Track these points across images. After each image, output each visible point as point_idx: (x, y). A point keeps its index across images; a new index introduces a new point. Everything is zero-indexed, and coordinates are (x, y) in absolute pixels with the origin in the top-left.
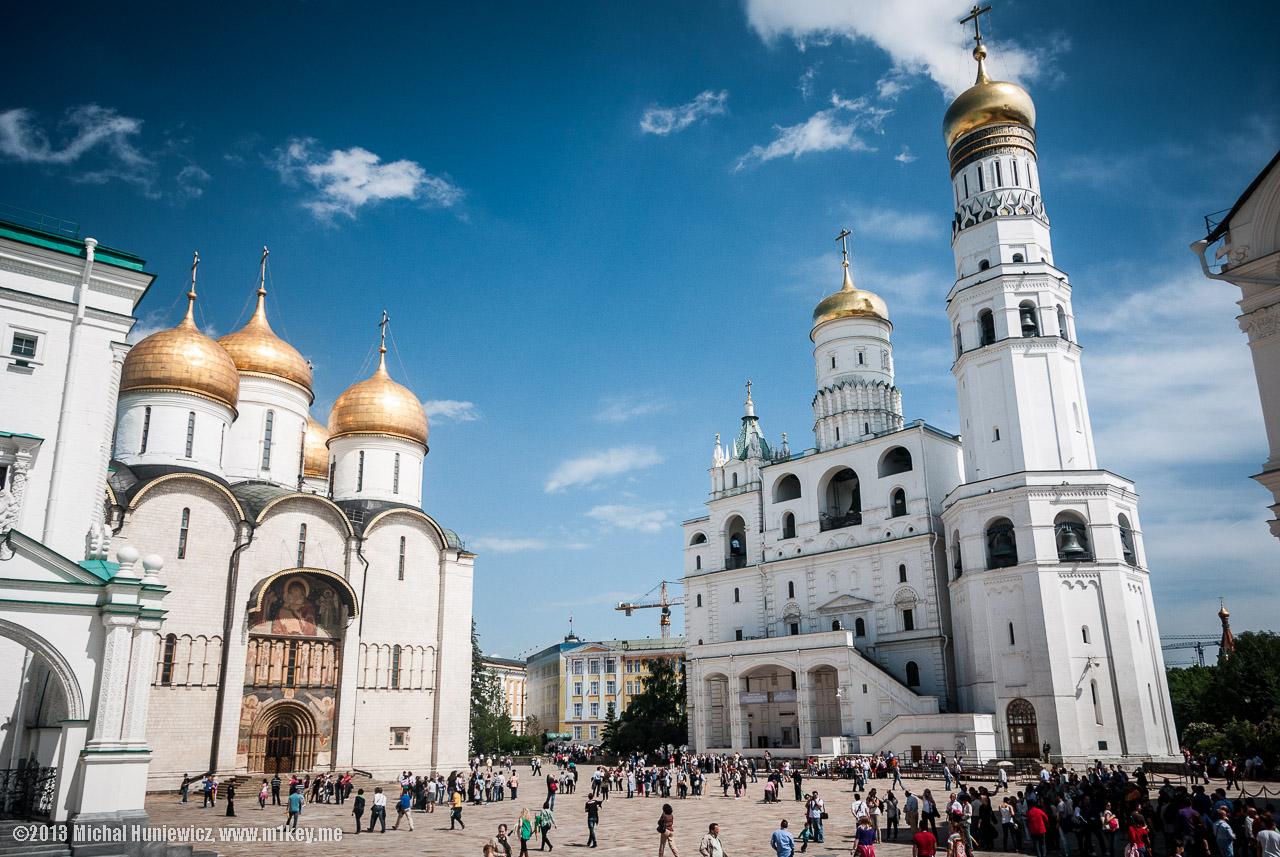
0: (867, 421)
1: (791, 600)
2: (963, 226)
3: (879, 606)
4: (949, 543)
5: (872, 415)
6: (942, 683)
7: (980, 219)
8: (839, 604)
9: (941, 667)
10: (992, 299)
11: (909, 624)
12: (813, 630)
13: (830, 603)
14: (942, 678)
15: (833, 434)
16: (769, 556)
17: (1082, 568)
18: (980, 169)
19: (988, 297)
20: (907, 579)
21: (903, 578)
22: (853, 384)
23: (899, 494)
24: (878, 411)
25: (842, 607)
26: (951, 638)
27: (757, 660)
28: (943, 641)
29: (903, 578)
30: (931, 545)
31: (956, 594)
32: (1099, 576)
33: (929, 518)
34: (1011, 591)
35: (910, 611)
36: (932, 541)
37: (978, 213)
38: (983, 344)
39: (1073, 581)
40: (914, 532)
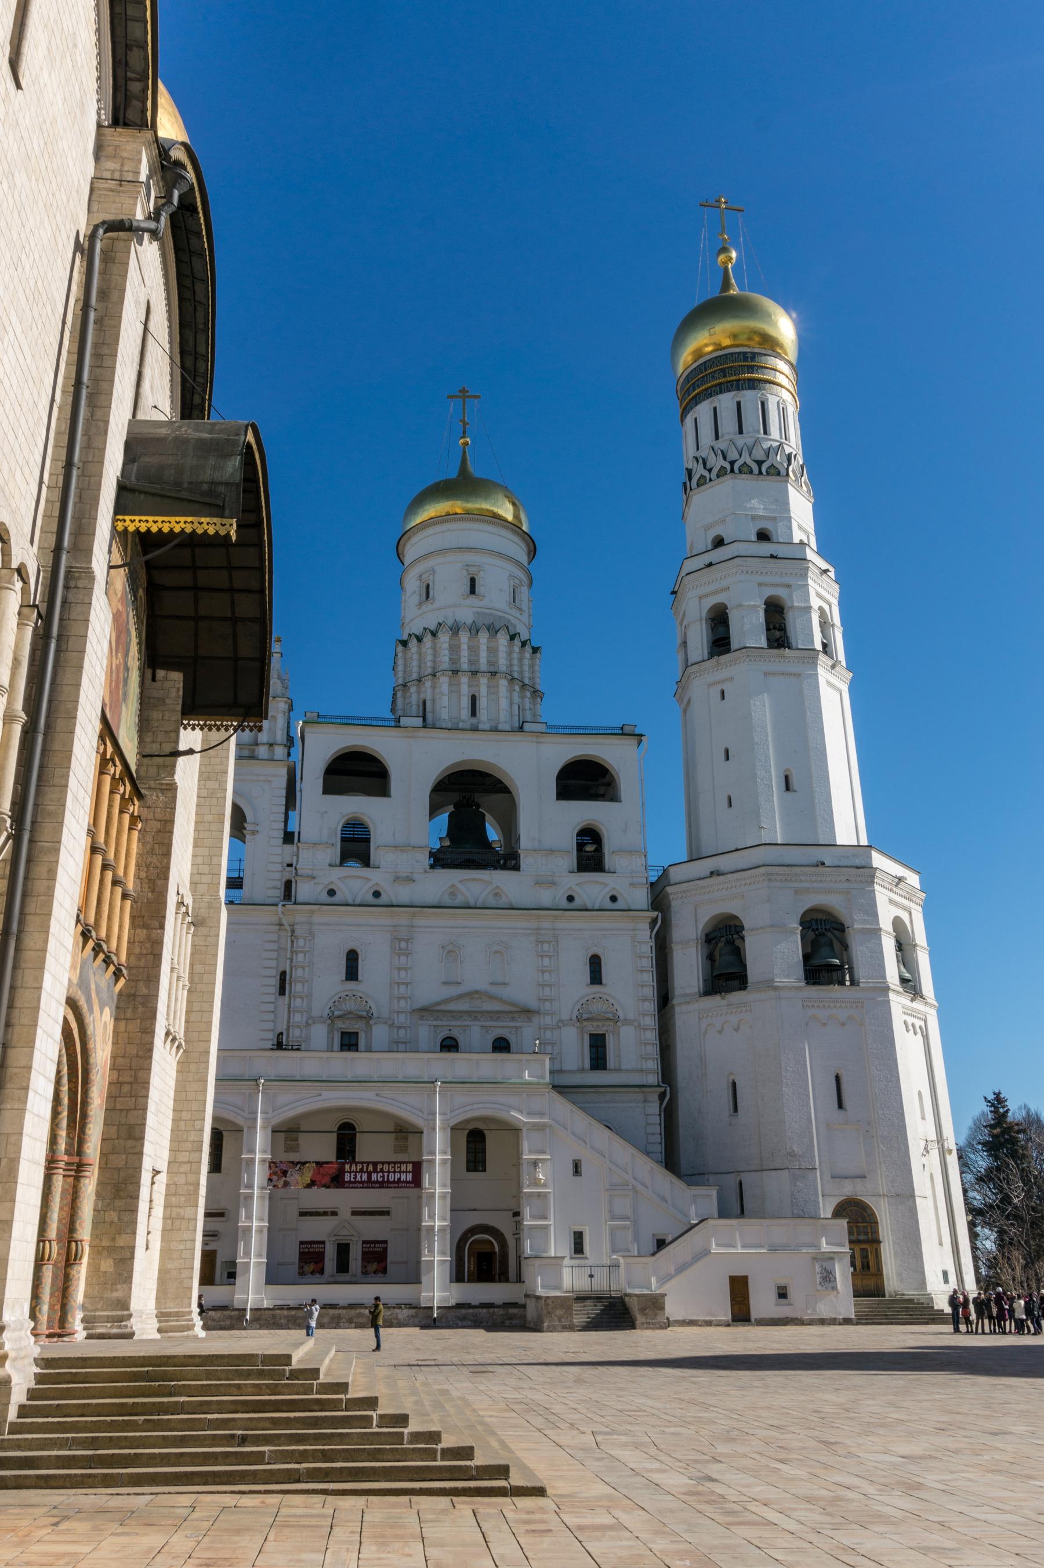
1: (351, 985)
2: (736, 468)
3: (548, 1020)
8: (463, 1006)
10: (789, 586)
11: (598, 1059)
12: (396, 1046)
13: (438, 1004)
15: (466, 702)
16: (303, 890)
17: (917, 1005)
19: (786, 580)
21: (596, 976)
25: (468, 1013)
27: (326, 1094)
28: (662, 1096)
29: (596, 976)
30: (651, 932)
34: (843, 1024)
37: (764, 462)
38: (771, 646)
39: (910, 1020)
40: (619, 905)
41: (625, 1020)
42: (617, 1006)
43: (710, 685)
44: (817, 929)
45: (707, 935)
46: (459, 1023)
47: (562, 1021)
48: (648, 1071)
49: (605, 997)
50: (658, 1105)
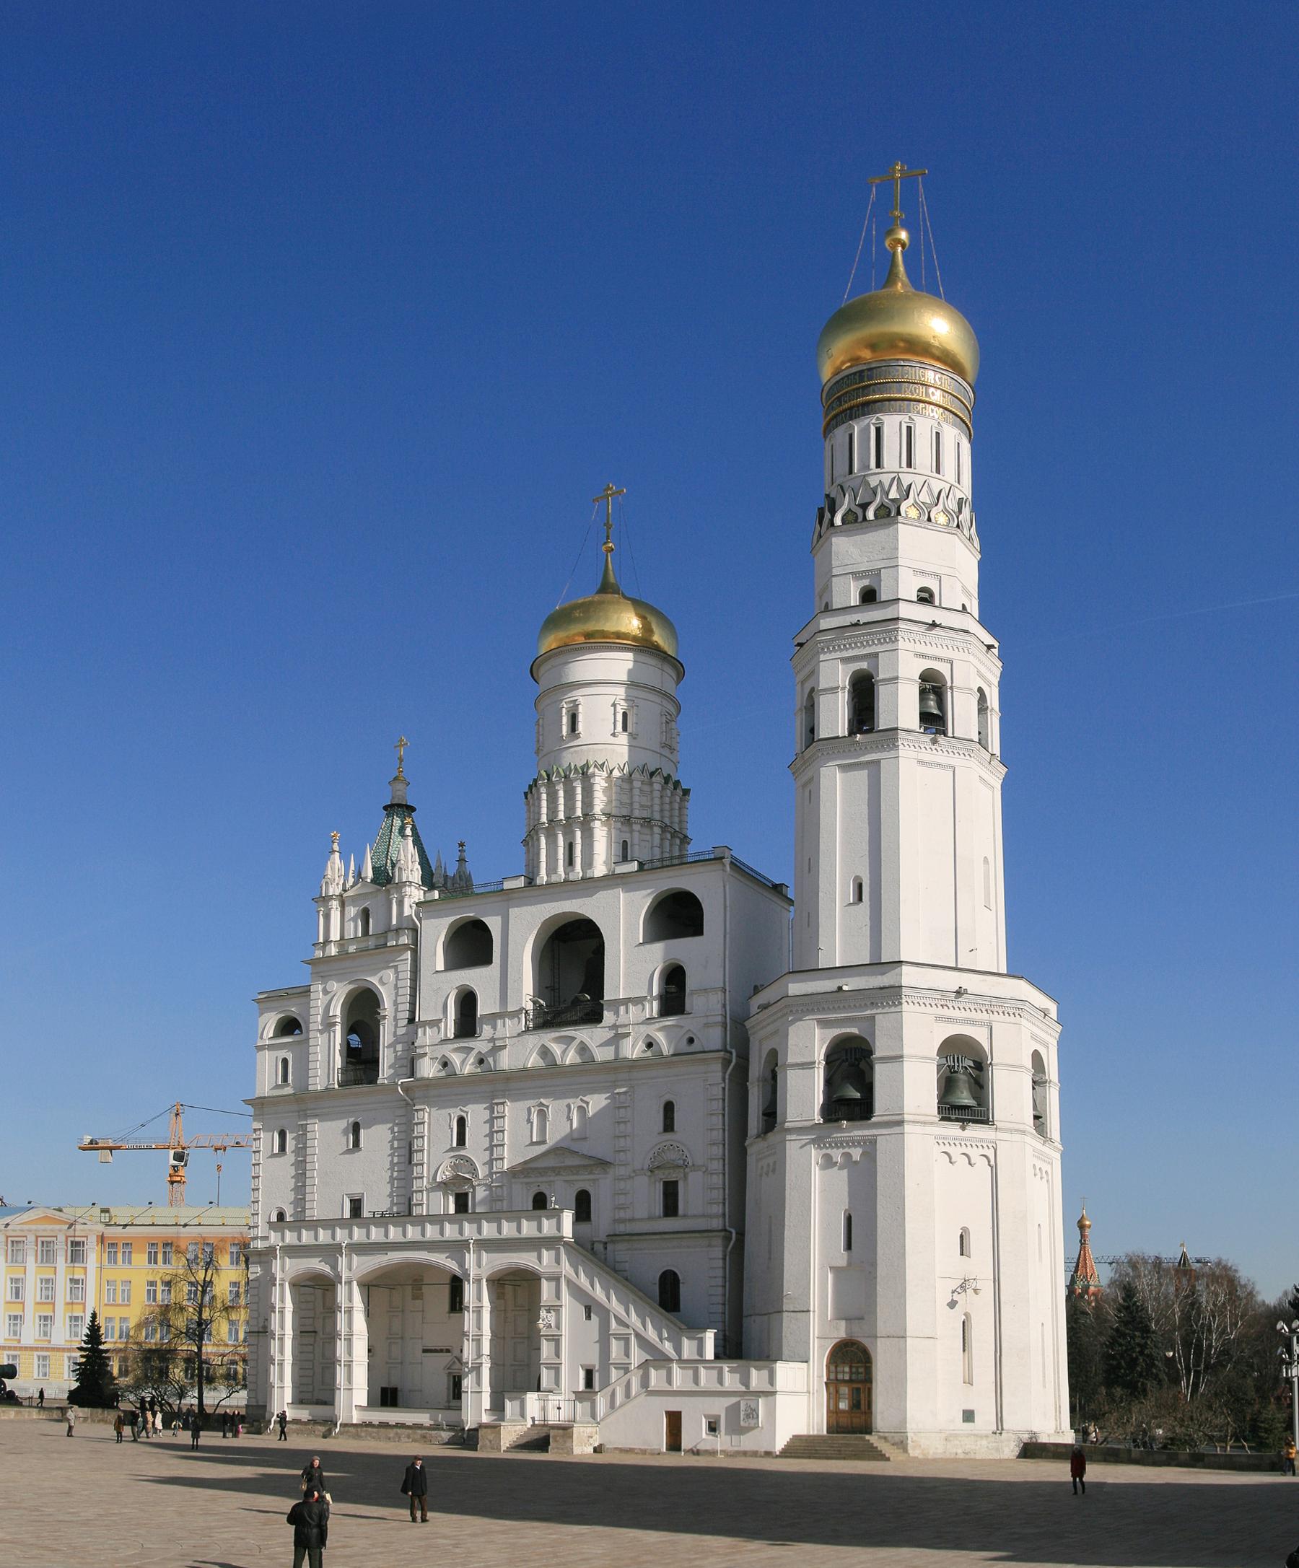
0: (627, 837)
3: (622, 1171)
4: (756, 1069)
5: (636, 827)
6: (720, 1308)
9: (720, 1281)
11: (671, 1208)
14: (719, 1299)
17: (974, 1131)
20: (676, 1128)
21: (669, 1126)
23: (674, 977)
24: (648, 822)
25: (553, 1169)
26: (741, 1235)
28: (727, 1239)
29: (669, 1126)
30: (724, 1073)
31: (758, 1161)
33: (724, 1025)
35: (677, 1182)
36: (726, 1063)
40: (696, 1047)
41: (693, 1165)
42: (686, 1152)
44: (847, 1059)
46: (544, 1179)
48: (715, 1216)
49: (675, 1144)
50: (721, 1249)
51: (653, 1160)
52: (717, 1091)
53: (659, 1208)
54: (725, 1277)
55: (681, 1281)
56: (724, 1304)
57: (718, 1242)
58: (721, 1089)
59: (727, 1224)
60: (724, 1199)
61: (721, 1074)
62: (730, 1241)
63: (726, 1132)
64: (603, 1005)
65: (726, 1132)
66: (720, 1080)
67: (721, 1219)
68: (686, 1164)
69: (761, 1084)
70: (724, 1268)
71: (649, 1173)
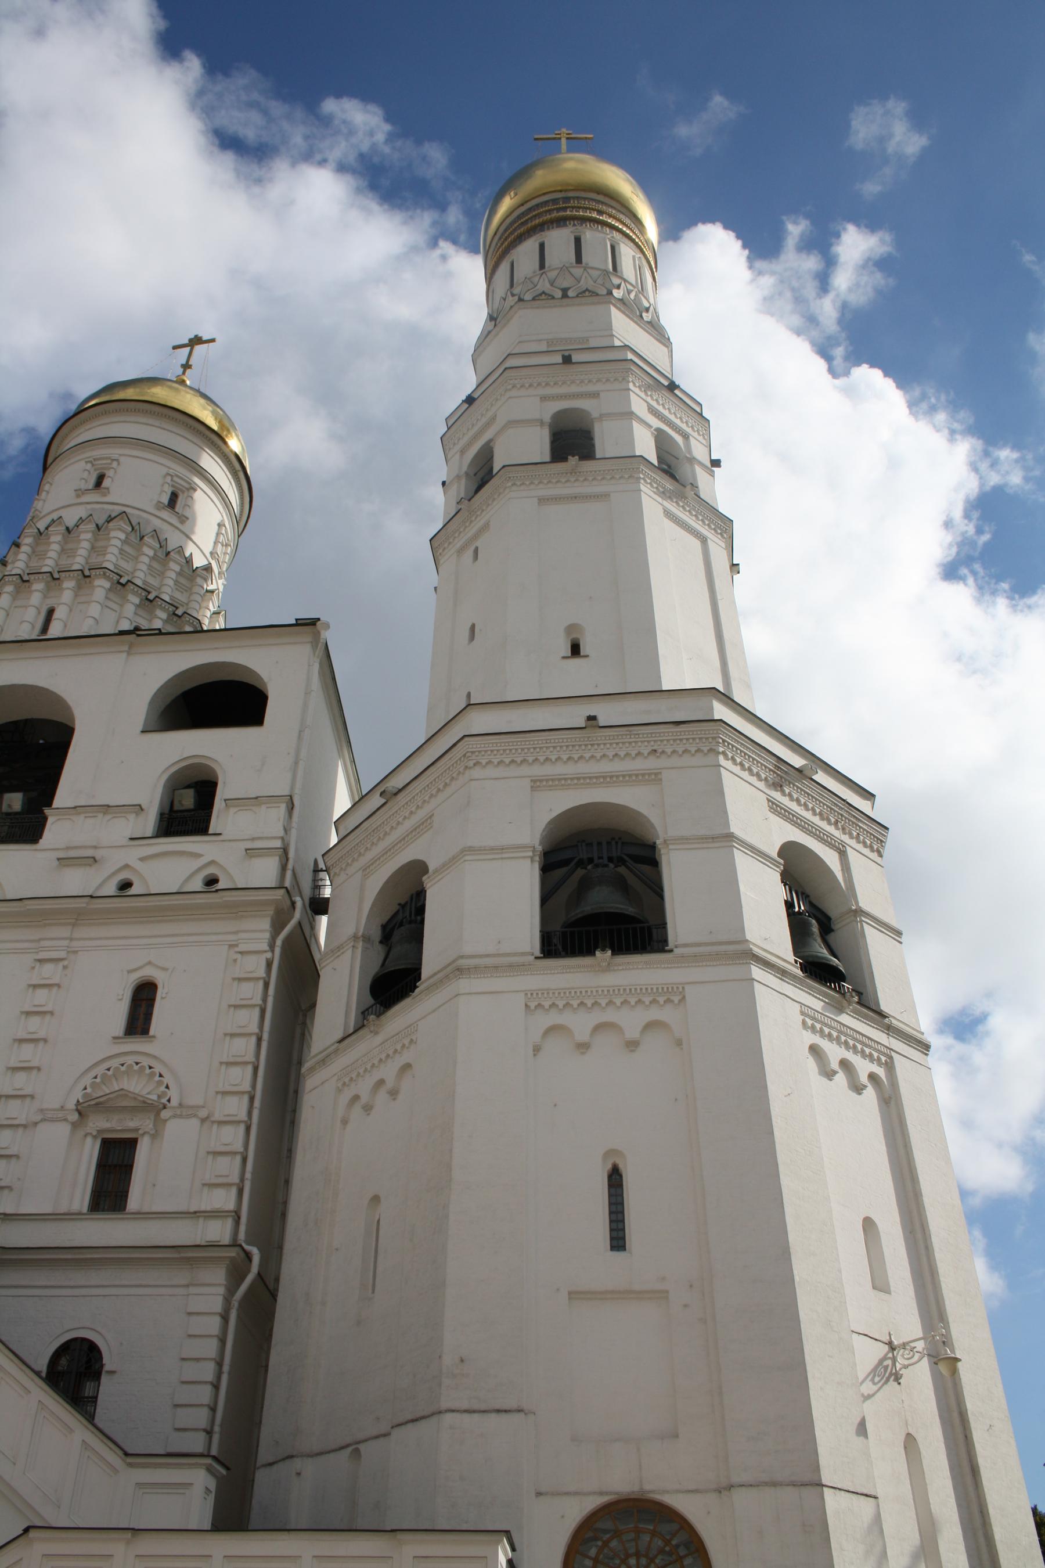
7: (570, 293)
9: (208, 1372)
10: (595, 395)
14: (200, 1418)
18: (578, 241)
19: (591, 388)
20: (152, 1032)
22: (137, 533)
28: (236, 1273)
32: (890, 1066)
34: (632, 1045)
41: (181, 1105)
42: (168, 1079)
43: (461, 551)
45: (384, 927)
47: (42, 1110)
49: (145, 1062)
50: (222, 1290)
51: (89, 1090)
52: (256, 966)
53: (81, 1198)
54: (220, 1364)
55: (106, 1368)
56: (209, 1432)
57: (218, 1276)
58: (263, 964)
59: (242, 1236)
60: (242, 1179)
61: (267, 935)
62: (242, 1278)
63: (264, 1045)
64: (45, 819)
65: (264, 1045)
66: (265, 947)
67: (229, 1223)
68: (164, 1101)
69: (360, 945)
70: (223, 1341)
71: (75, 1116)
